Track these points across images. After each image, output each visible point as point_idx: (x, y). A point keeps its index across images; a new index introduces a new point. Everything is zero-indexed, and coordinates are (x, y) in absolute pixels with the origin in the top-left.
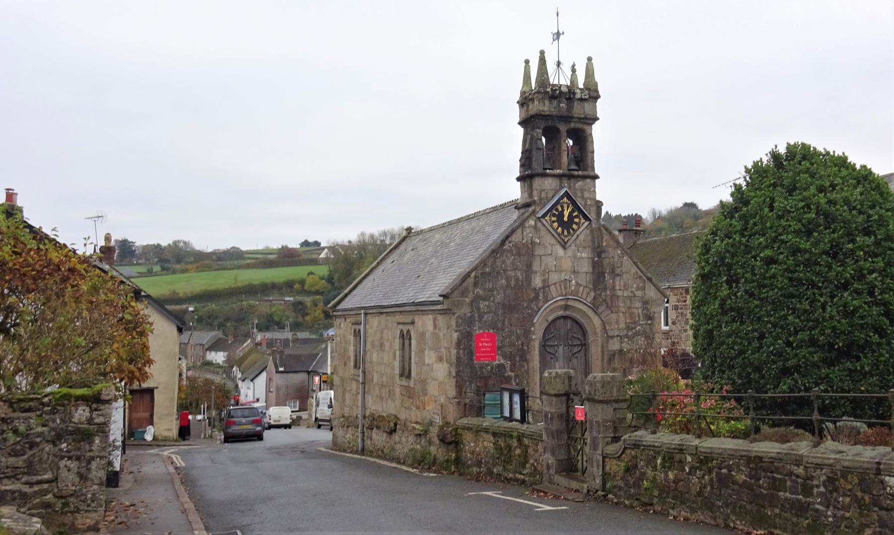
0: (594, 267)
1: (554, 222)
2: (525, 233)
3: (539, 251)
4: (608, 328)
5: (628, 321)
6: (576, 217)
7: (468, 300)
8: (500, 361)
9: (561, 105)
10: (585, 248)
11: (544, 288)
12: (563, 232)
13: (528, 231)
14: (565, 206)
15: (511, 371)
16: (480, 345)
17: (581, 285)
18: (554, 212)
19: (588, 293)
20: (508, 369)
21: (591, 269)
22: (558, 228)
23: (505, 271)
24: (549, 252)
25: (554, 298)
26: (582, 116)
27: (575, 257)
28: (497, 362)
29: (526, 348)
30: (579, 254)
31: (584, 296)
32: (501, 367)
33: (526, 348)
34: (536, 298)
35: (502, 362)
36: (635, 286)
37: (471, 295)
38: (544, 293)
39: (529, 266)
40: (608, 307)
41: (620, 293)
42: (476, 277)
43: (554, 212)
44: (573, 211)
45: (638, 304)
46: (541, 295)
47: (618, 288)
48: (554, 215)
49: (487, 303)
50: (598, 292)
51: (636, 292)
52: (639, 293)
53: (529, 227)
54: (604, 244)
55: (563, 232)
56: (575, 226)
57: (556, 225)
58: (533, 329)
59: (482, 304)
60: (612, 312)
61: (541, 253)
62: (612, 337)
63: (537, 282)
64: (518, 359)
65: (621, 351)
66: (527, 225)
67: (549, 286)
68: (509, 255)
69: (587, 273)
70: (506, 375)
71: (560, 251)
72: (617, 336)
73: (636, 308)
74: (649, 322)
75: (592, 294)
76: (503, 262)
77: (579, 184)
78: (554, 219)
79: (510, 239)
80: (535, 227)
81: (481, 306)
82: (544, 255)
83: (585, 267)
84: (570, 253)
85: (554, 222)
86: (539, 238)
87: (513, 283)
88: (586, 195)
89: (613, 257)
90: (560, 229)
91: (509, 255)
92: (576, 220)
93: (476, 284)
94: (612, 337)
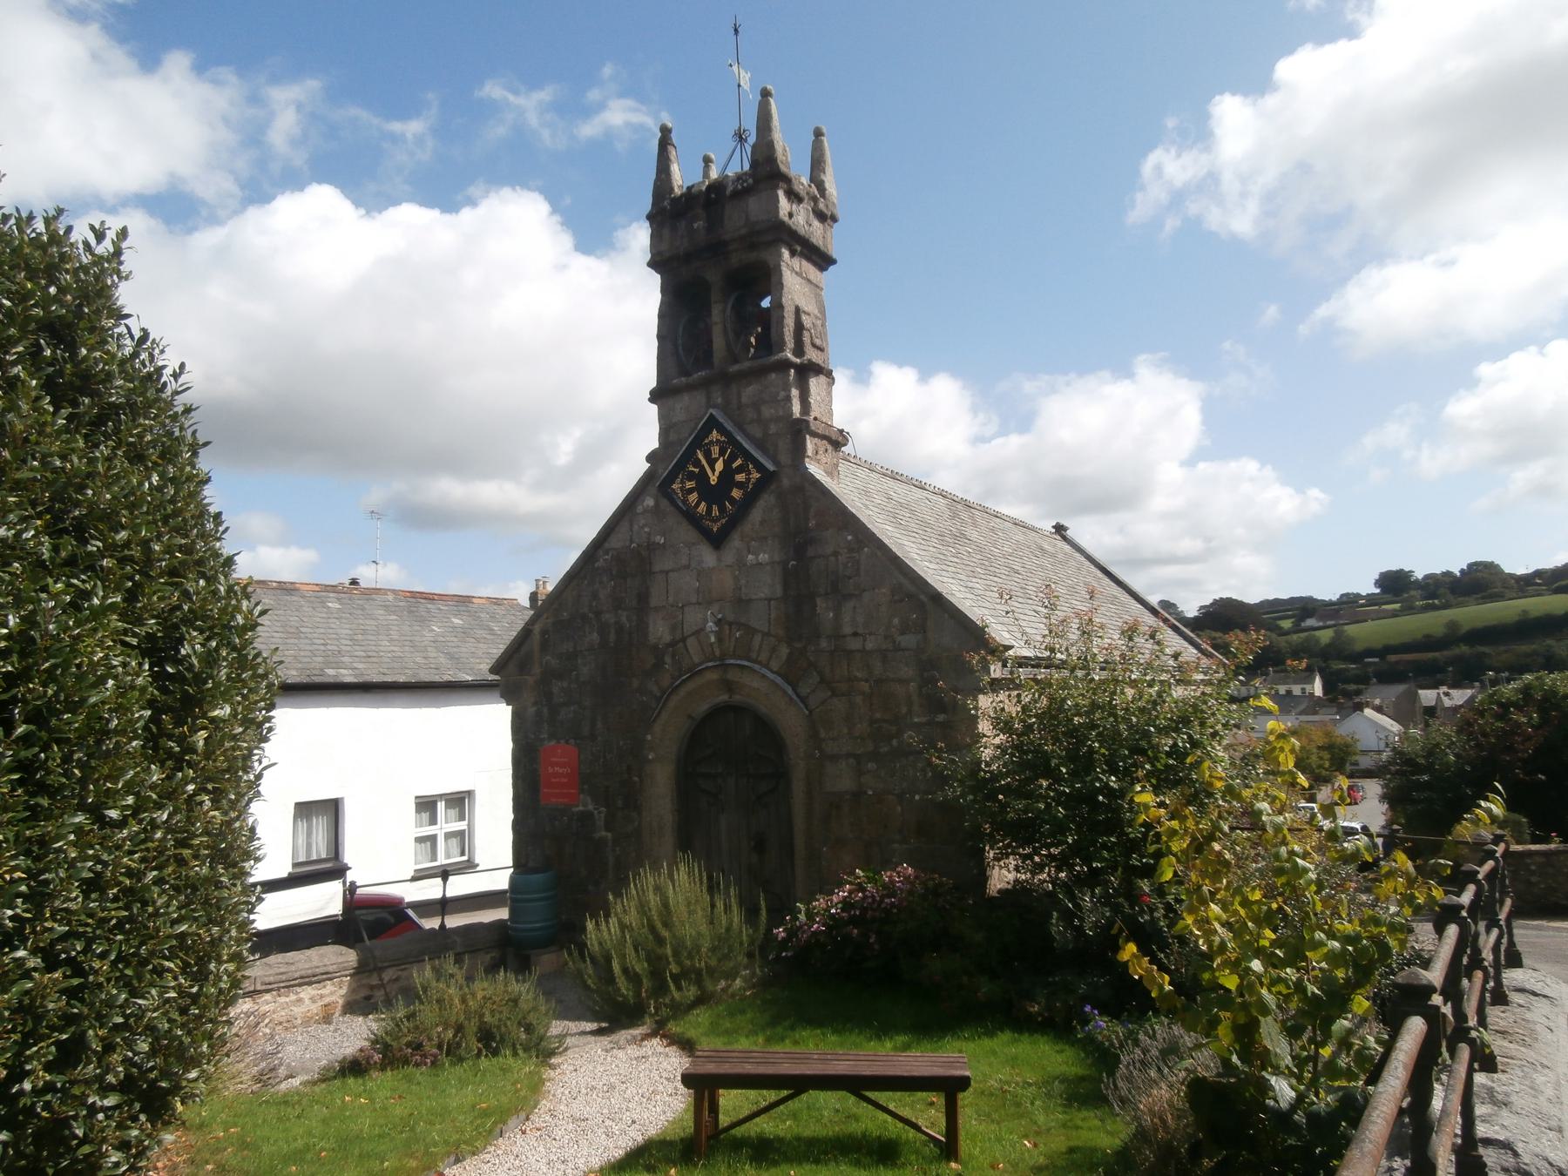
0: (786, 585)
1: (691, 491)
2: (636, 527)
3: (662, 563)
4: (823, 734)
5: (878, 715)
6: (740, 470)
7: (530, 680)
8: (585, 805)
9: (695, 225)
10: (765, 538)
11: (673, 644)
12: (709, 510)
13: (642, 522)
14: (715, 450)
15: (607, 829)
16: (550, 770)
17: (754, 631)
18: (692, 469)
19: (774, 650)
20: (600, 823)
21: (779, 592)
22: (698, 505)
23: (598, 614)
24: (684, 561)
25: (755, 661)
26: (743, 231)
27: (741, 563)
28: (581, 808)
29: (636, 779)
30: (750, 557)
31: (763, 657)
32: (586, 817)
33: (636, 779)
34: (659, 665)
35: (591, 807)
36: (896, 621)
37: (537, 670)
38: (673, 656)
39: (643, 597)
40: (822, 681)
41: (854, 644)
42: (544, 632)
43: (692, 469)
44: (733, 458)
45: (907, 671)
46: (668, 659)
47: (847, 630)
48: (691, 476)
49: (565, 684)
50: (798, 645)
51: (899, 638)
52: (909, 640)
53: (645, 511)
54: (812, 523)
55: (709, 510)
56: (736, 493)
57: (693, 497)
58: (649, 737)
59: (557, 687)
60: (834, 694)
61: (668, 565)
62: (834, 758)
63: (659, 630)
64: (620, 803)
65: (858, 795)
66: (640, 509)
67: (684, 640)
68: (605, 579)
69: (770, 600)
70: (597, 835)
71: (708, 557)
72: (849, 755)
73: (901, 681)
74: (941, 718)
75: (784, 651)
76: (595, 596)
77: (749, 392)
78: (690, 485)
79: (606, 545)
80: (656, 510)
81: (555, 690)
82: (673, 571)
83: (766, 586)
84: (729, 556)
85: (691, 491)
86: (663, 535)
87: (612, 637)
88: (767, 412)
89: (836, 554)
90: (703, 507)
91: (605, 579)
92: (740, 477)
93: (544, 646)
94: (834, 758)
